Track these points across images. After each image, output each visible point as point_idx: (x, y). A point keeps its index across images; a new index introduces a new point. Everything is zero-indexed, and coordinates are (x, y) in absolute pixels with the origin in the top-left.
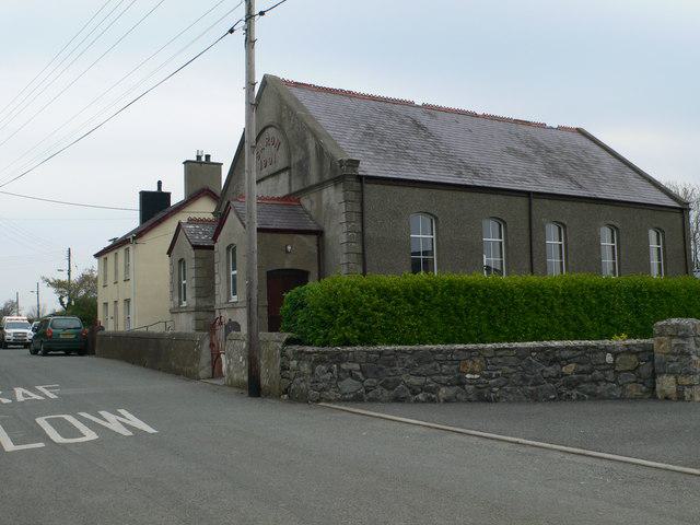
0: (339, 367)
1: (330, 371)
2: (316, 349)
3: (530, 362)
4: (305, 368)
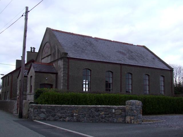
0: (40, 110)
1: (38, 111)
2: (35, 105)
3: (92, 111)
4: (32, 110)
